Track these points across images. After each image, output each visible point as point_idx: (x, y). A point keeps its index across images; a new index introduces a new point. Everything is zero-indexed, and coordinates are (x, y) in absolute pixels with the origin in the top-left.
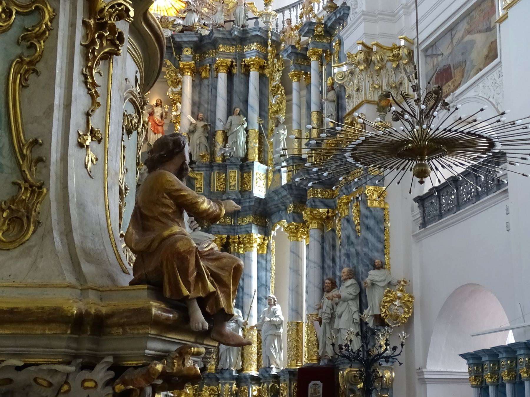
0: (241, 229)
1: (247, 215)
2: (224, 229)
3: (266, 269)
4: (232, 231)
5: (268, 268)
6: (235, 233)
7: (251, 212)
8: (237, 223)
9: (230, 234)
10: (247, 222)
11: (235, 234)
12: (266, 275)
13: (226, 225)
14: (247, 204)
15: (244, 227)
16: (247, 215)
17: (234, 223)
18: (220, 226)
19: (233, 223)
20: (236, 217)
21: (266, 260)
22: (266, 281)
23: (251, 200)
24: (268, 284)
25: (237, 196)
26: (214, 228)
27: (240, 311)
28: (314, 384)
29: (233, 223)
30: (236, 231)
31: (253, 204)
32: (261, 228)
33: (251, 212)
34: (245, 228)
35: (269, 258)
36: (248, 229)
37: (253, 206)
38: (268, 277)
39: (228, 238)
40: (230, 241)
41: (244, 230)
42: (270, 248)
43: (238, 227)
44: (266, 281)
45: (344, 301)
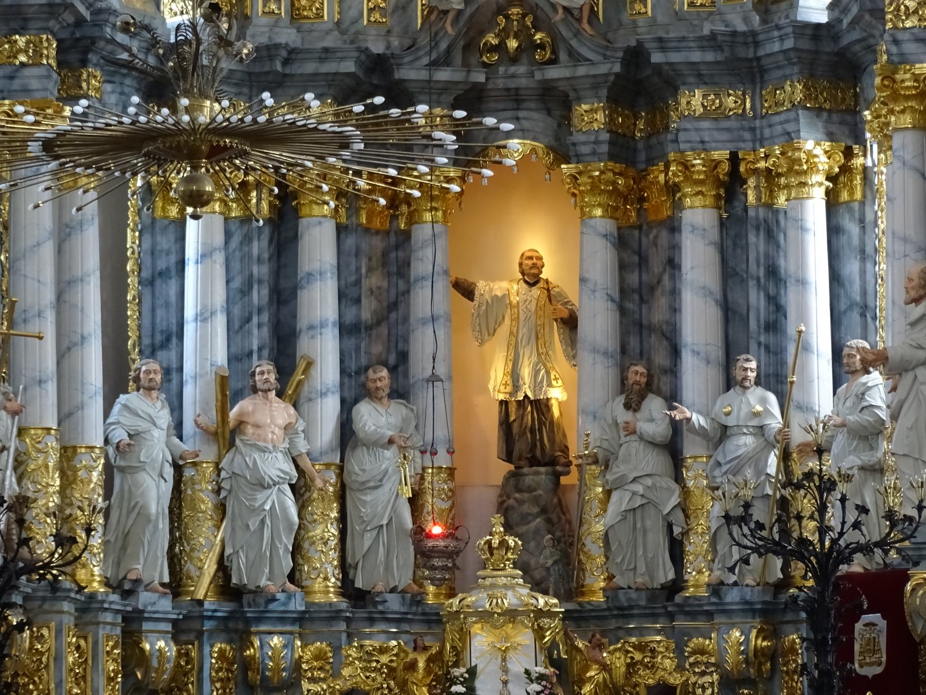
0: (770, 126)
1: (785, 77)
2: (718, 129)
3: (863, 251)
4: (747, 135)
5: (869, 250)
6: (754, 141)
7: (796, 69)
8: (762, 107)
9: (742, 145)
10: (788, 105)
11: (758, 145)
12: (863, 272)
13: (728, 117)
14: (776, 47)
15: (777, 119)
16: (786, 80)
17: (753, 107)
18: (705, 124)
19: (748, 105)
20: (758, 90)
21: (862, 221)
22: (864, 293)
23: (782, 32)
24: (871, 304)
25: (746, 20)
26: (685, 130)
27: (772, 398)
28: (866, 625)
29: (748, 105)
30: (758, 136)
31: (789, 44)
32: (835, 117)
33: (796, 69)
34: (781, 123)
35: (869, 217)
36: (790, 127)
37: (794, 49)
38: (870, 277)
39: (734, 159)
40: (742, 169)
41: (778, 129)
42: (872, 182)
43: (765, 122)
44: (864, 293)
45: (906, 371)
